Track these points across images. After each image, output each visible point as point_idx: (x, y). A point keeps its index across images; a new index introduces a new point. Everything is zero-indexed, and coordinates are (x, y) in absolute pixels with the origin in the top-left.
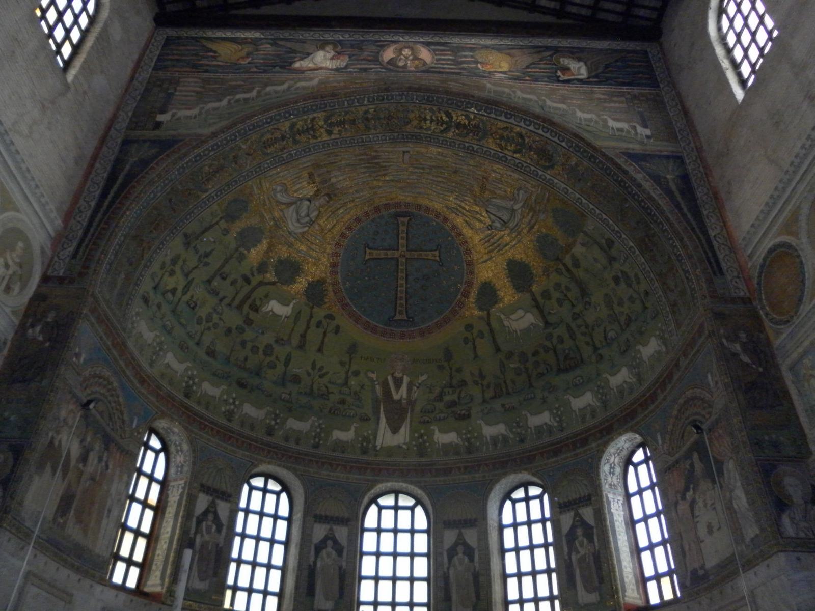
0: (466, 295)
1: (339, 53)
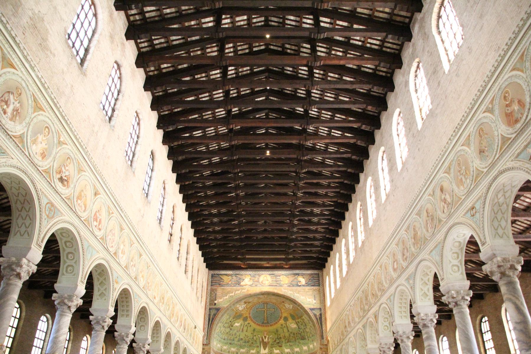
1: (250, 279)
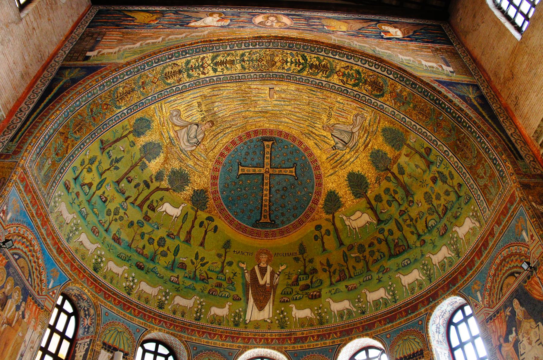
0: (316, 202)
